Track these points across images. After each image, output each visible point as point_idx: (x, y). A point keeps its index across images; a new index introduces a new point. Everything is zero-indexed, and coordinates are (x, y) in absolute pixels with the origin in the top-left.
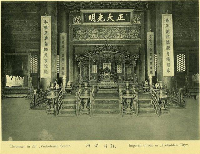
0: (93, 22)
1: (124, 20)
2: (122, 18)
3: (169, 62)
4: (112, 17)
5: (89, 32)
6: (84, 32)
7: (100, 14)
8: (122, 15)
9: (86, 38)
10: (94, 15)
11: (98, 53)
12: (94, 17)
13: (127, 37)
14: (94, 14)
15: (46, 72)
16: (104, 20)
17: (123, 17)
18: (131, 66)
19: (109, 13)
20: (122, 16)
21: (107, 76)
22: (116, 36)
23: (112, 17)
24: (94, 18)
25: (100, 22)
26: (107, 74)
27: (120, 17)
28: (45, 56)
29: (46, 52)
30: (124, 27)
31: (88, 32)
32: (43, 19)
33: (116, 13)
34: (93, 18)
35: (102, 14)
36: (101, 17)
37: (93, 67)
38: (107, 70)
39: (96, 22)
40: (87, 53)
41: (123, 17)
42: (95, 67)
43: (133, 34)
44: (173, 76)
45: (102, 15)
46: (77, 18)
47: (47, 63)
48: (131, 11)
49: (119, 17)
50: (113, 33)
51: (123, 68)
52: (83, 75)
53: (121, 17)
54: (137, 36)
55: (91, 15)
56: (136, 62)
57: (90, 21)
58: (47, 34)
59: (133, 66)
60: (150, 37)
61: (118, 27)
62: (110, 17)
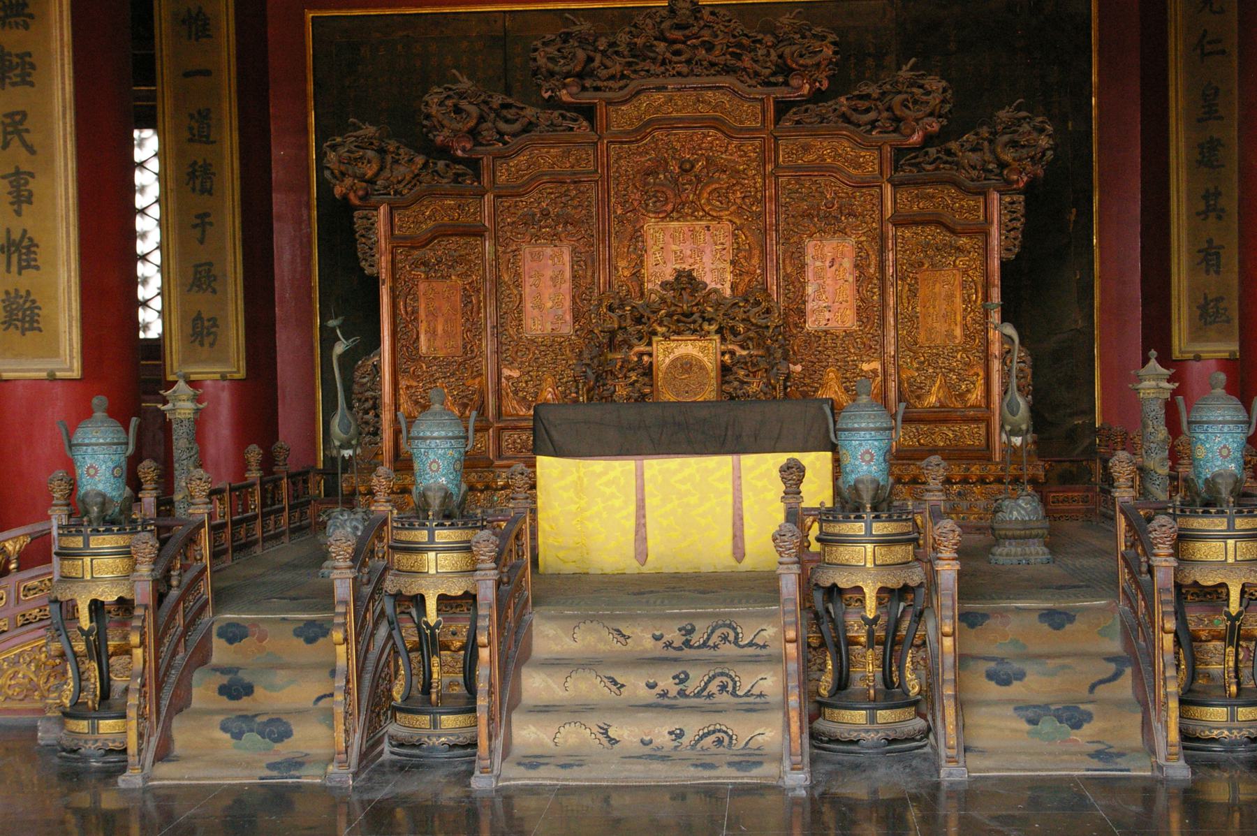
11: (587, 98)
18: (958, 249)
21: (686, 365)
26: (687, 348)
28: (6, 145)
37: (527, 265)
38: (686, 306)
40: (458, 110)
42: (549, 273)
47: (28, 221)
52: (416, 357)
56: (1020, 208)
59: (986, 234)
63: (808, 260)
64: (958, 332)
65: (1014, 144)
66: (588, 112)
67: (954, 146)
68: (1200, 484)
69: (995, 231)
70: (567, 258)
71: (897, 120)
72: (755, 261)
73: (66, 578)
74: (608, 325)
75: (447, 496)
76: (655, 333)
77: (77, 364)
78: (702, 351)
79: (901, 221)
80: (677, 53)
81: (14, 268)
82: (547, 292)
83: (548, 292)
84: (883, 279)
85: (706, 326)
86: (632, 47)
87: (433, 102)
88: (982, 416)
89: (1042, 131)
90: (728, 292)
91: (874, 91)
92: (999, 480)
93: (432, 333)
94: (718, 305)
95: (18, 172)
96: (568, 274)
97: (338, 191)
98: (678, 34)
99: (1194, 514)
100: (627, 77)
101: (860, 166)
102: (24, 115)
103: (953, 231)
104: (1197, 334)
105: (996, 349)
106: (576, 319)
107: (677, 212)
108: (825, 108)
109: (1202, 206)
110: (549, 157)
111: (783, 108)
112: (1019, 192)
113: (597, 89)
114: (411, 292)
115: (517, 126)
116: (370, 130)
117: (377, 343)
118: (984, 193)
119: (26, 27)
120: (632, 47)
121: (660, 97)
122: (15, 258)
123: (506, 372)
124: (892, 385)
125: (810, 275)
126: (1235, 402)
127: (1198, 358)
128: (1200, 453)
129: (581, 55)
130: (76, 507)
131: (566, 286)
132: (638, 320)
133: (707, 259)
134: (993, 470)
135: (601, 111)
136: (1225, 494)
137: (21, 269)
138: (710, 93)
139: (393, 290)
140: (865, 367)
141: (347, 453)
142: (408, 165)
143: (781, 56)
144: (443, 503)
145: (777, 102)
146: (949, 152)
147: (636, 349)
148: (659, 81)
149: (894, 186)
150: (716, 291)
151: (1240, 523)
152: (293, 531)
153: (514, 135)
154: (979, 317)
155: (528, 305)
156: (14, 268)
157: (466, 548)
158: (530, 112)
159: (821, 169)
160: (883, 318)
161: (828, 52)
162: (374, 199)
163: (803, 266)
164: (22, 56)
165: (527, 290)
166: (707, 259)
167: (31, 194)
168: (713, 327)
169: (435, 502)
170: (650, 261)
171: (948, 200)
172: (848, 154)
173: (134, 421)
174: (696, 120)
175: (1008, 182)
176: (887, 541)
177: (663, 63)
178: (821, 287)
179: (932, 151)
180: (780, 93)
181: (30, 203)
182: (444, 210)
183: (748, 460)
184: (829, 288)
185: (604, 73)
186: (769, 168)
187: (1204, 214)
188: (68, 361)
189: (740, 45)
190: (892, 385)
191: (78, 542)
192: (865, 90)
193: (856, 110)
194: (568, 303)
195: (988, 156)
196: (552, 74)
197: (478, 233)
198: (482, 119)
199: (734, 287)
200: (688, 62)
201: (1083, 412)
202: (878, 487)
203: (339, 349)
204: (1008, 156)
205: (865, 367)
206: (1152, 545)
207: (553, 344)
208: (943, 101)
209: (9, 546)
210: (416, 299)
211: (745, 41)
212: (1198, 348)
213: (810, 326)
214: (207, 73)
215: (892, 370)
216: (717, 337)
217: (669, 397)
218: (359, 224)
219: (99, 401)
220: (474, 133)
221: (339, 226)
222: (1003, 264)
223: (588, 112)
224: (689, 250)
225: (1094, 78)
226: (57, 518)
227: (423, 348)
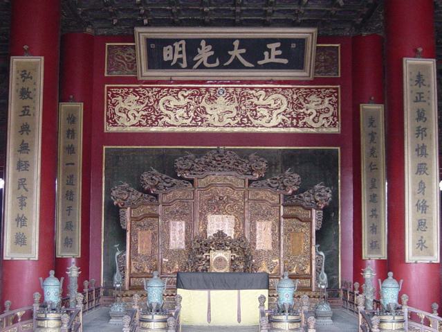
0: (177, 66)
1: (285, 61)
2: (277, 57)
3: (424, 216)
4: (243, 51)
5: (161, 103)
6: (143, 103)
7: (203, 43)
8: (278, 45)
9: (150, 122)
10: (181, 46)
12: (180, 52)
13: (292, 123)
14: (183, 42)
15: (21, 240)
16: (217, 63)
17: (279, 52)
19: (234, 40)
20: (277, 49)
21: (220, 259)
22: (255, 117)
23: (243, 51)
24: (180, 56)
25: (202, 67)
26: (220, 254)
27: (269, 50)
29: (23, 174)
30: (283, 89)
31: (158, 101)
32: (15, 60)
33: (259, 40)
34: (177, 56)
35: (209, 41)
36: (205, 53)
38: (220, 241)
39: (190, 67)
40: (152, 179)
41: (279, 52)
43: (315, 113)
44: (438, 261)
45: (210, 47)
46: (122, 54)
47: (25, 211)
48: (306, 33)
49: (266, 54)
50: (243, 108)
51: (276, 234)
52: (136, 254)
53: (274, 53)
54: (327, 118)
55: (170, 47)
57: (167, 65)
58: (28, 114)
59: (311, 222)
60: (372, 123)
61: (262, 88)
62: (236, 53)
63: (257, 228)
64: (302, 251)
65: (320, 195)
66: (192, 181)
67: (302, 195)
68: (385, 306)
69: (314, 221)
70: (184, 225)
71: (285, 186)
72: (241, 228)
73: (39, 327)
74: (196, 247)
75: (158, 305)
76: (211, 249)
77: (37, 255)
78: (226, 255)
79: (285, 217)
80: (219, 164)
81: (19, 226)
82: (177, 235)
83: (177, 236)
84: (280, 234)
85: (226, 248)
86: (206, 162)
87: (145, 176)
88: (309, 277)
89: (328, 192)
90: (233, 238)
91: (278, 178)
92: (314, 297)
93: (142, 247)
94: (231, 241)
95: (22, 197)
96: (184, 230)
97: (115, 203)
98: (219, 159)
99: (383, 315)
100: (203, 171)
101: (273, 200)
102: (25, 179)
103: (301, 221)
104: (369, 253)
105: (314, 257)
106: (186, 244)
107: (218, 212)
108: (263, 182)
109: (371, 214)
110: (179, 194)
111: (250, 182)
112: (321, 209)
113: (194, 174)
114: (136, 234)
115: (170, 185)
116: (126, 185)
117: (125, 250)
118: (311, 210)
119: (27, 153)
120: (206, 162)
121: (213, 177)
122: (20, 223)
123: (164, 260)
124: (282, 267)
125: (257, 232)
126: (395, 281)
127: (370, 259)
128: (385, 296)
129: (190, 164)
130: (43, 305)
131: (183, 234)
132: (206, 245)
133: (226, 226)
134: (313, 294)
135: (196, 181)
136: (392, 309)
137: (21, 226)
138: (228, 177)
139: (130, 234)
140: (274, 261)
141: (118, 286)
142: (135, 196)
143: (250, 166)
144: (157, 307)
145: (249, 180)
146: (300, 197)
147: (205, 254)
148: (214, 173)
149: (284, 206)
150: (230, 237)
151: (396, 318)
152: (96, 307)
153: (168, 187)
154: (309, 247)
155: (171, 239)
156: (19, 226)
157: (165, 321)
158: (174, 180)
159: (263, 201)
160: (280, 246)
161: (264, 165)
162: (125, 206)
163: (256, 230)
164: (26, 162)
165: (171, 235)
166: (226, 226)
167: (26, 203)
168: (229, 248)
169: (154, 307)
170: (209, 226)
171: (300, 211)
172: (270, 197)
173: (62, 278)
174: (225, 184)
175: (318, 206)
176: (293, 322)
177: (215, 167)
178: (261, 237)
179: (295, 196)
180: (250, 177)
181: (25, 206)
182: (147, 209)
183: (242, 292)
184: (263, 236)
185: (196, 169)
186: (246, 199)
187: (372, 216)
188: (34, 254)
189: (238, 162)
190: (282, 267)
191: (43, 316)
192: (275, 177)
193: (272, 183)
194: (184, 239)
195: (312, 199)
196: (181, 169)
197: (157, 216)
198: (159, 182)
199: (235, 236)
200: (222, 167)
201: (335, 275)
202: (290, 305)
203: (117, 254)
204: (318, 199)
205: (274, 261)
206: (372, 325)
207: (179, 251)
208: (299, 181)
209: (19, 314)
210: (137, 237)
211: (240, 162)
212: (371, 256)
213: (257, 248)
214: (73, 164)
215: (282, 262)
216: (230, 251)
217: (214, 270)
218: (121, 213)
219: (52, 273)
220: (156, 186)
221: (114, 213)
222: (317, 231)
223: (192, 181)
224: (220, 223)
225: (339, 174)
226: (36, 307)
227: (139, 252)
